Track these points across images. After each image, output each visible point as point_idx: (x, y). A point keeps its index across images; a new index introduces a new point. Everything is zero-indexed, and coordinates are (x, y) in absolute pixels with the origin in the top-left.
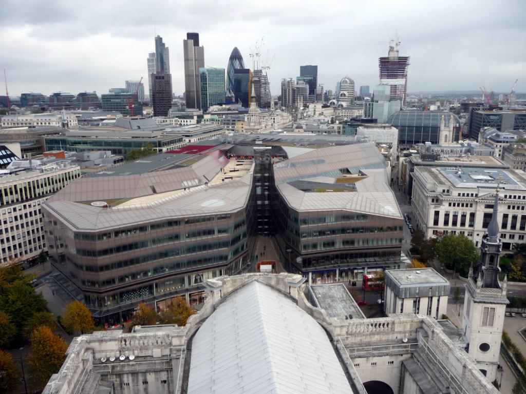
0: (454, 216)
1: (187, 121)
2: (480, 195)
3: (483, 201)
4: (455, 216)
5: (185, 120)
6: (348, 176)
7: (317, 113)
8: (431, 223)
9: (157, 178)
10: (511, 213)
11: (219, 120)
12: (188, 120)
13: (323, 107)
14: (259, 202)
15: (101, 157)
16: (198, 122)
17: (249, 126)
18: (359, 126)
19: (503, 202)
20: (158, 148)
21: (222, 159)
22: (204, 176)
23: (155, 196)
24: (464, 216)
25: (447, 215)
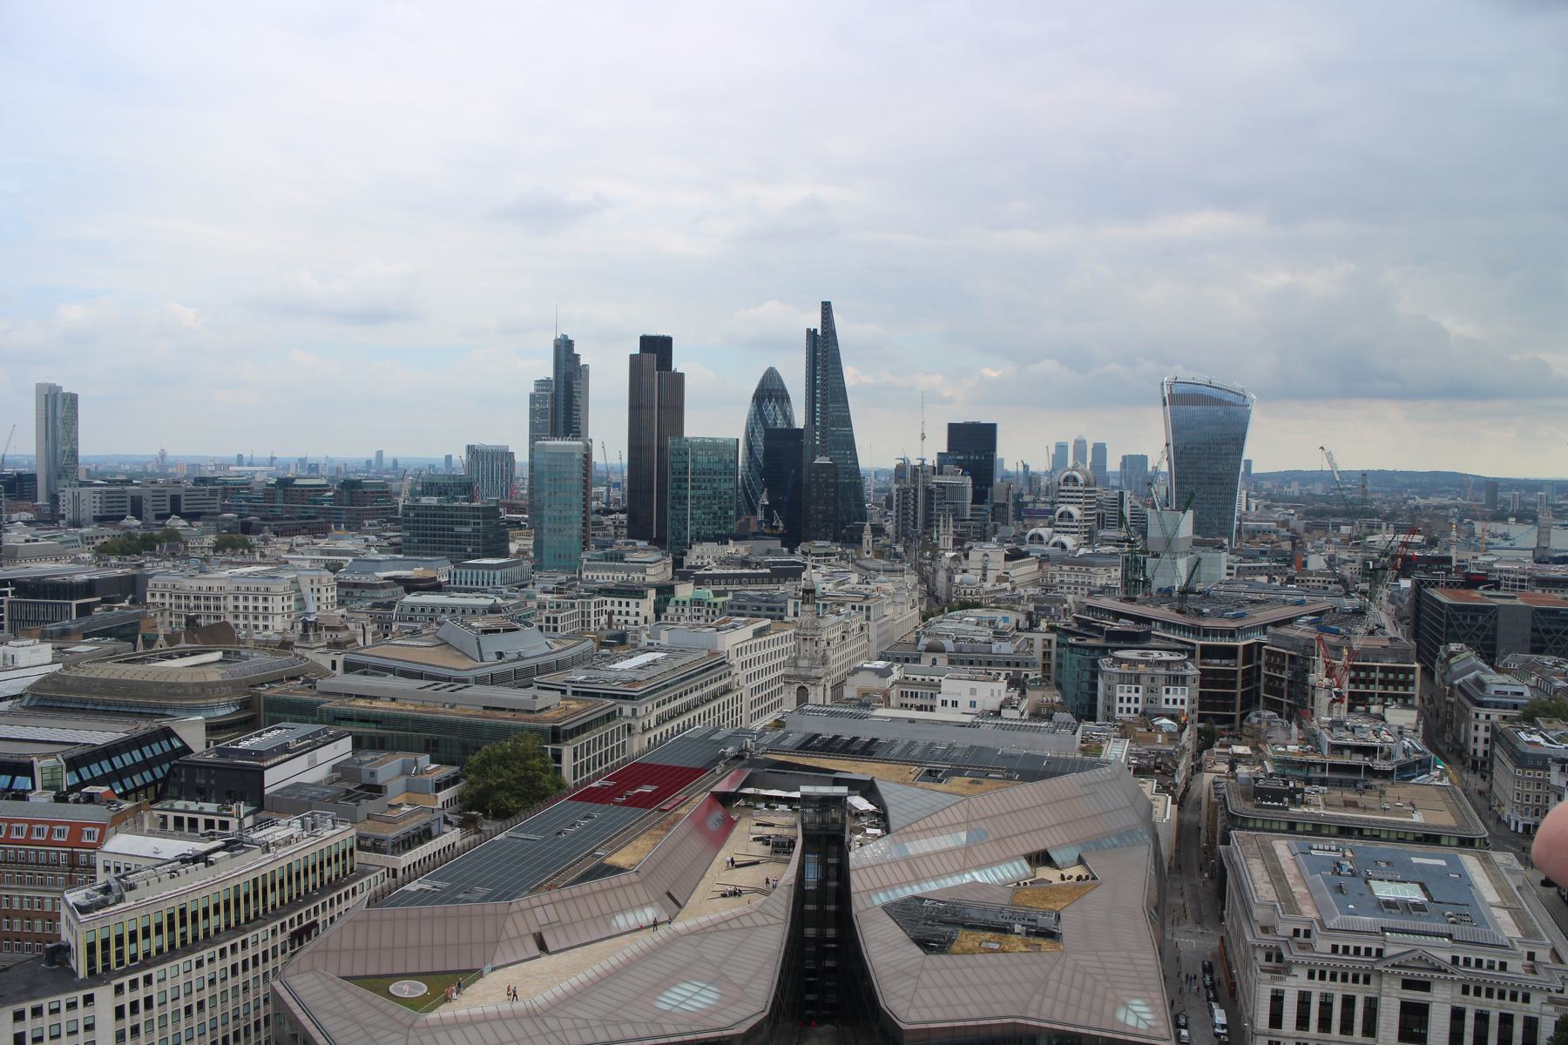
0: (1321, 1003)
1: (628, 604)
2: (1388, 952)
3: (1396, 971)
4: (1326, 1006)
5: (624, 601)
6: (1045, 873)
7: (991, 575)
8: (1263, 1020)
9: (550, 908)
10: (1472, 1005)
11: (715, 605)
12: (633, 602)
13: (1008, 558)
14: (810, 932)
15: (405, 771)
16: (659, 611)
17: (796, 666)
18: (1104, 651)
19: (1449, 977)
20: (549, 747)
21: (718, 813)
22: (669, 895)
23: (545, 959)
24: (1348, 1002)
25: (1304, 1000)
